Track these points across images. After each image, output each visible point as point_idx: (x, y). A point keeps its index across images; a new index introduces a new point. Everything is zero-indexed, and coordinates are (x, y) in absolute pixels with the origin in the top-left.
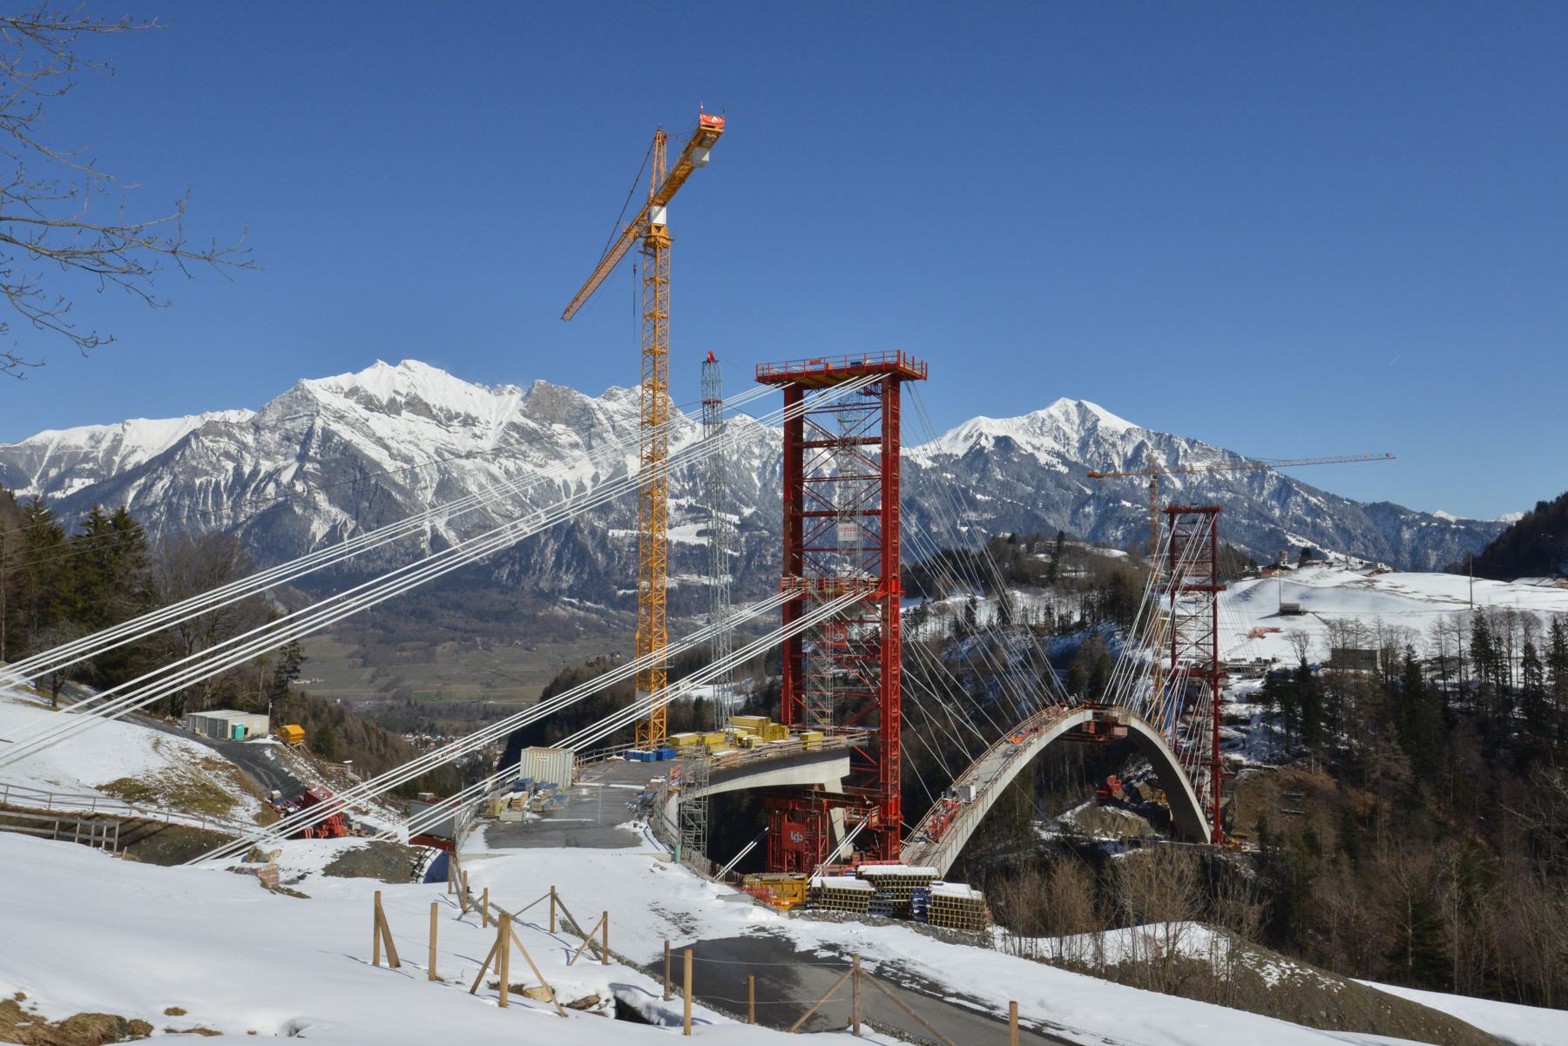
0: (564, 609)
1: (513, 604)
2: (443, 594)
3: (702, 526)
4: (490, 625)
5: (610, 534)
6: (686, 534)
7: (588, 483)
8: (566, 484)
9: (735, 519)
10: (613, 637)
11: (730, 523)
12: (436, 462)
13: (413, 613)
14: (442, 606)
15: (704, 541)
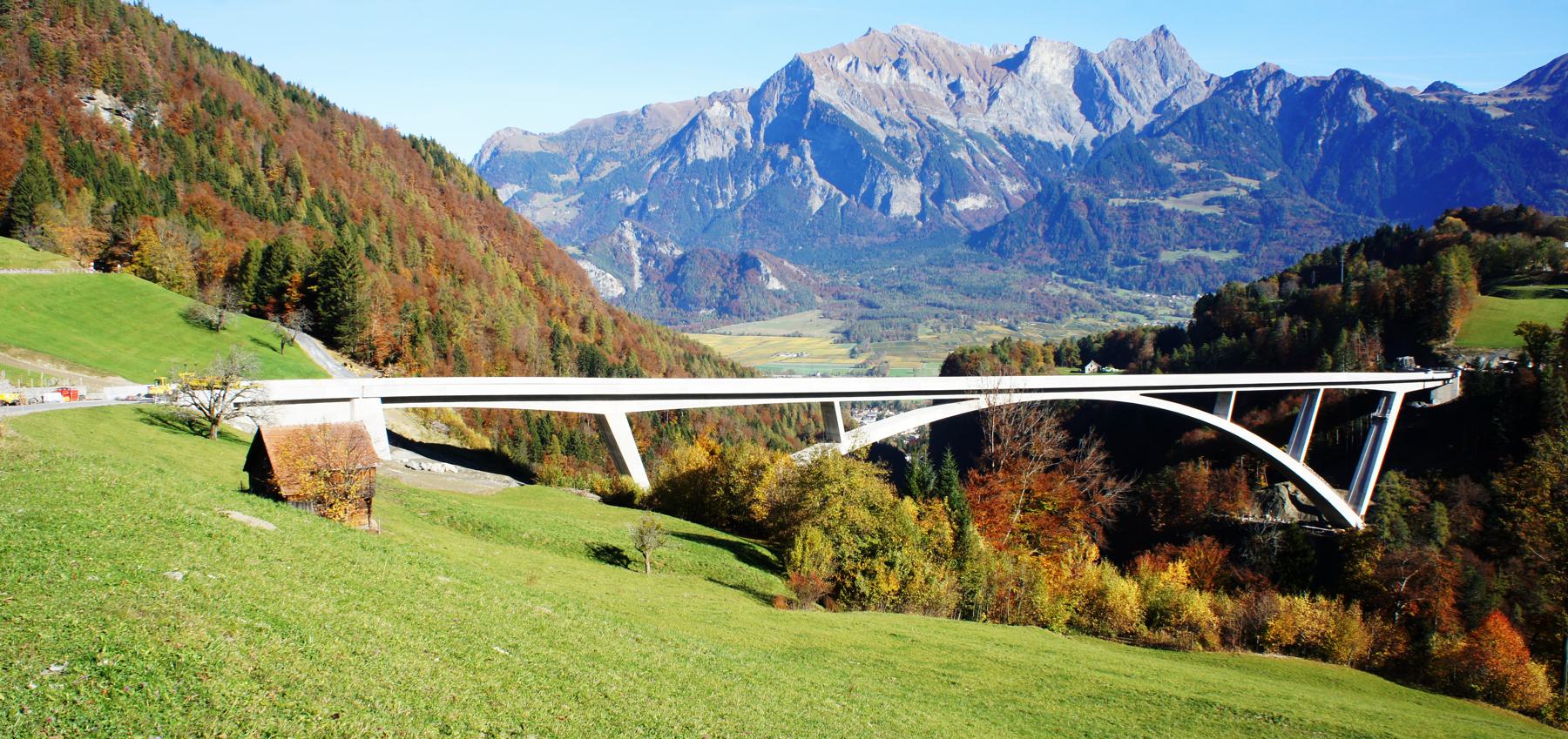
0: (1057, 287)
1: (1003, 280)
2: (932, 269)
3: (1212, 193)
4: (976, 303)
5: (1110, 204)
6: (1192, 203)
7: (1089, 147)
8: (1065, 148)
9: (1255, 184)
10: (1104, 317)
11: (1246, 188)
12: (928, 130)
13: (901, 288)
14: (931, 282)
15: (1216, 210)
